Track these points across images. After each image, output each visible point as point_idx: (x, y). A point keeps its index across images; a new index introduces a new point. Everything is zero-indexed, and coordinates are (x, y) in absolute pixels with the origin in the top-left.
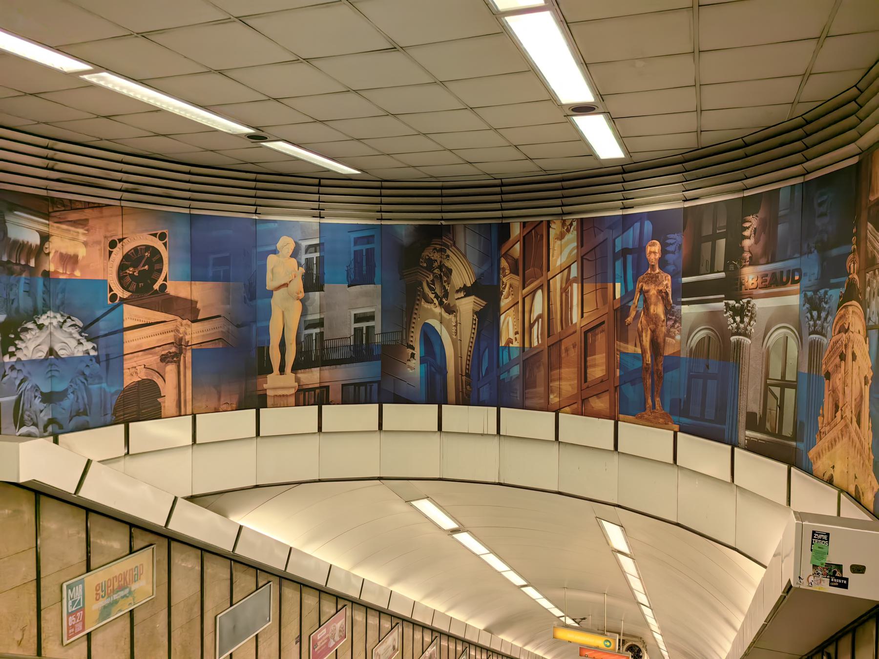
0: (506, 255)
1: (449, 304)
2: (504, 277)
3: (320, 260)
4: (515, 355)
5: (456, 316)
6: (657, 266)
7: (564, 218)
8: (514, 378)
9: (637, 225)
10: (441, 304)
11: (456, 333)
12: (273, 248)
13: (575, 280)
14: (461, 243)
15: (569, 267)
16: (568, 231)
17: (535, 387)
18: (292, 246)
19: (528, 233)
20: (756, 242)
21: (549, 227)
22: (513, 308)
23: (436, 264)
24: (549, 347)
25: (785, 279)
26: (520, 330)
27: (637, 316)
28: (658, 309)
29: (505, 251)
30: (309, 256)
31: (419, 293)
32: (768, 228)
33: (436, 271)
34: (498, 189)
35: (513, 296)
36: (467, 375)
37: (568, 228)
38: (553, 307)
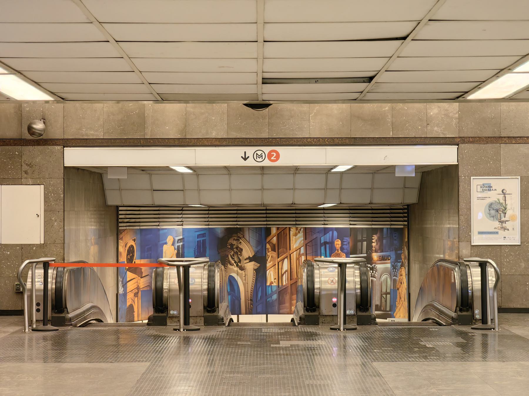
0: (269, 242)
1: (241, 266)
2: (268, 252)
3: (183, 245)
4: (274, 289)
5: (245, 271)
6: (340, 250)
7: (297, 226)
8: (274, 300)
9: (331, 232)
10: (237, 265)
11: (245, 279)
12: (164, 242)
13: (303, 254)
14: (247, 236)
15: (300, 248)
16: (299, 232)
17: (285, 304)
18: (172, 240)
19: (279, 233)
20: (377, 244)
21: (290, 230)
22: (273, 267)
23: (235, 247)
24: (291, 285)
25: (386, 258)
26: (277, 278)
29: (269, 240)
30: (179, 244)
31: (227, 261)
32: (380, 240)
33: (235, 250)
34: (264, 212)
35: (273, 262)
36: (251, 300)
37: (299, 231)
38: (292, 267)
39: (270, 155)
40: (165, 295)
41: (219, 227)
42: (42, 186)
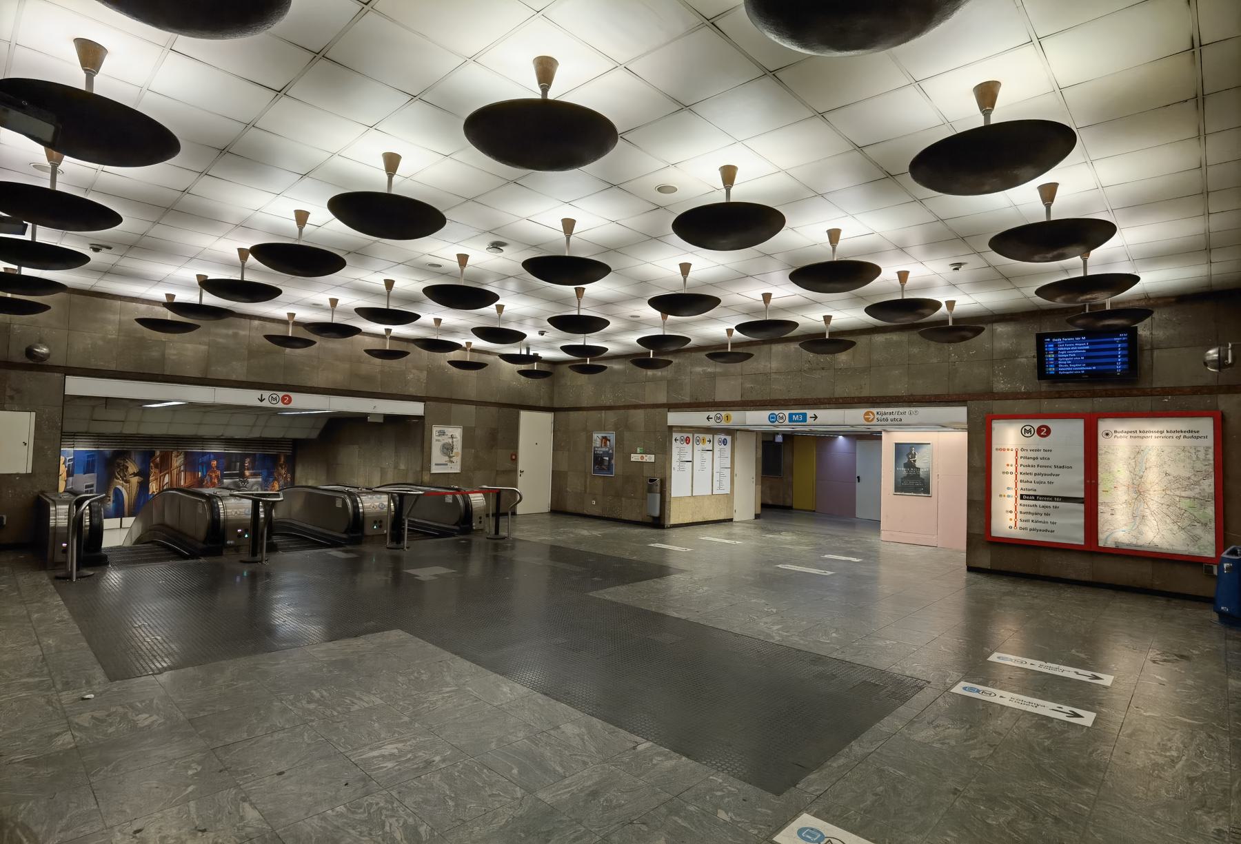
0: (153, 462)
3: (74, 463)
10: (123, 480)
14: (133, 457)
27: (207, 482)
28: (216, 481)
32: (253, 462)
39: (283, 399)
40: (222, 524)
41: (107, 450)
42: (33, 414)
